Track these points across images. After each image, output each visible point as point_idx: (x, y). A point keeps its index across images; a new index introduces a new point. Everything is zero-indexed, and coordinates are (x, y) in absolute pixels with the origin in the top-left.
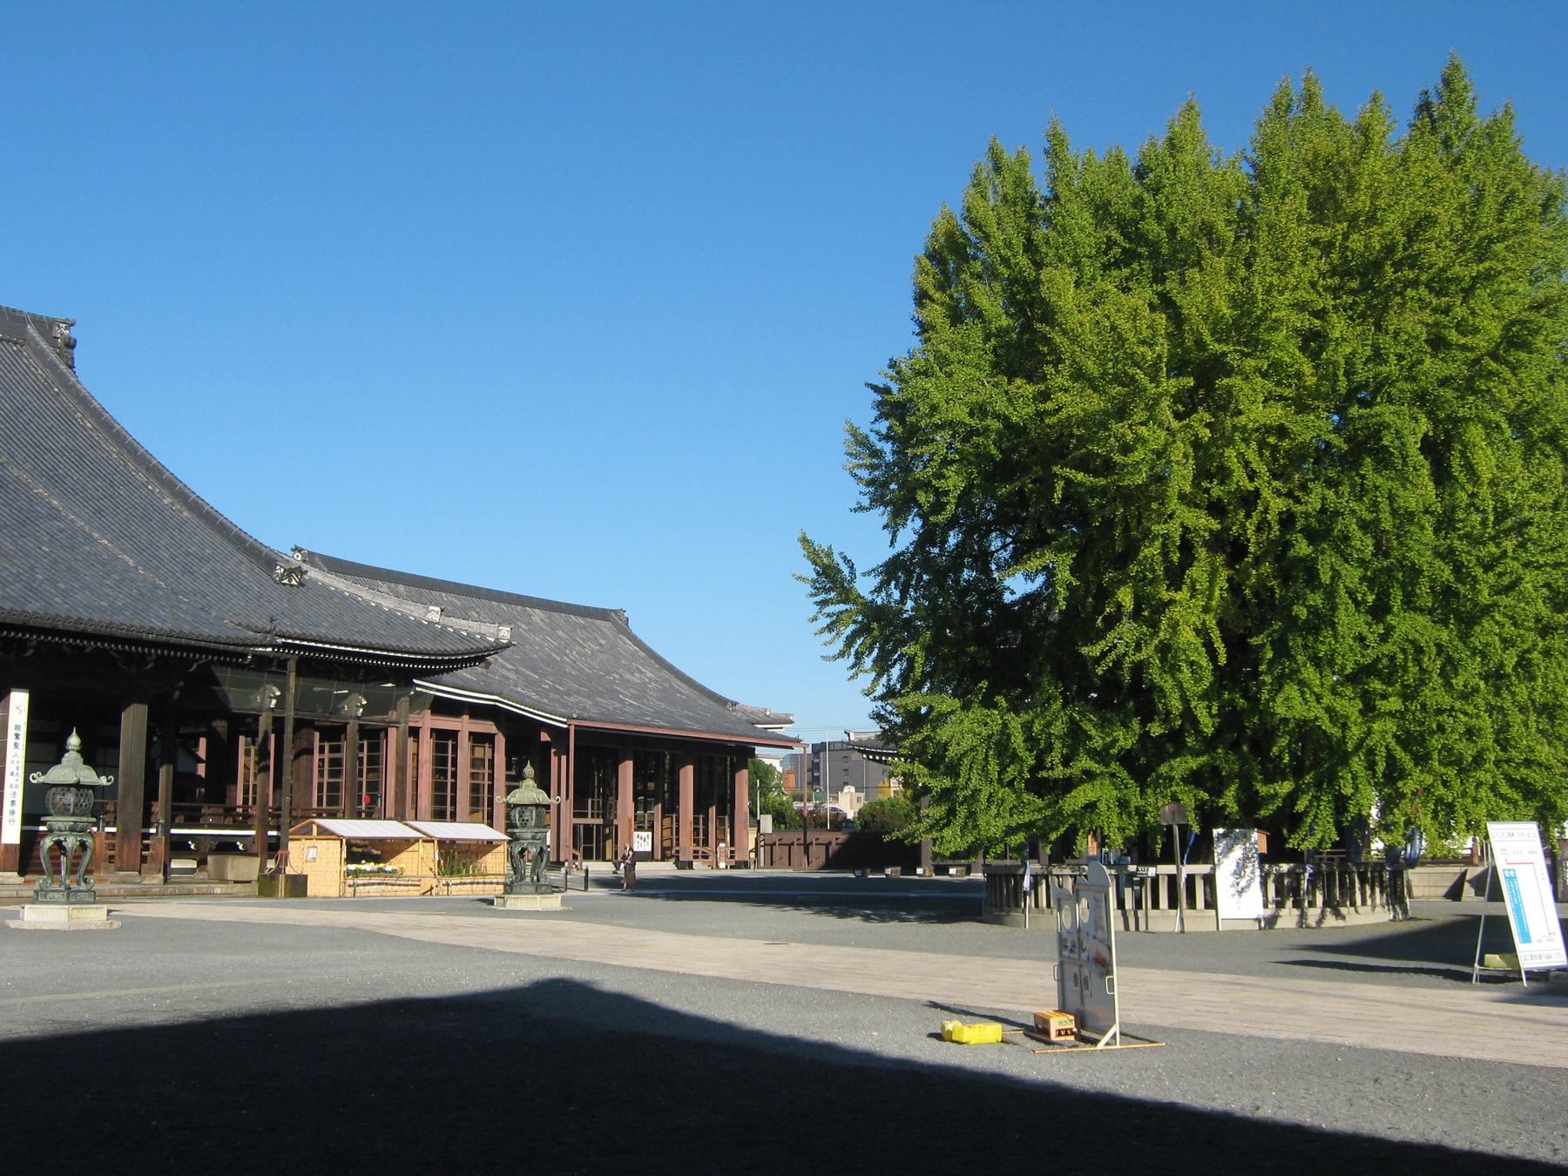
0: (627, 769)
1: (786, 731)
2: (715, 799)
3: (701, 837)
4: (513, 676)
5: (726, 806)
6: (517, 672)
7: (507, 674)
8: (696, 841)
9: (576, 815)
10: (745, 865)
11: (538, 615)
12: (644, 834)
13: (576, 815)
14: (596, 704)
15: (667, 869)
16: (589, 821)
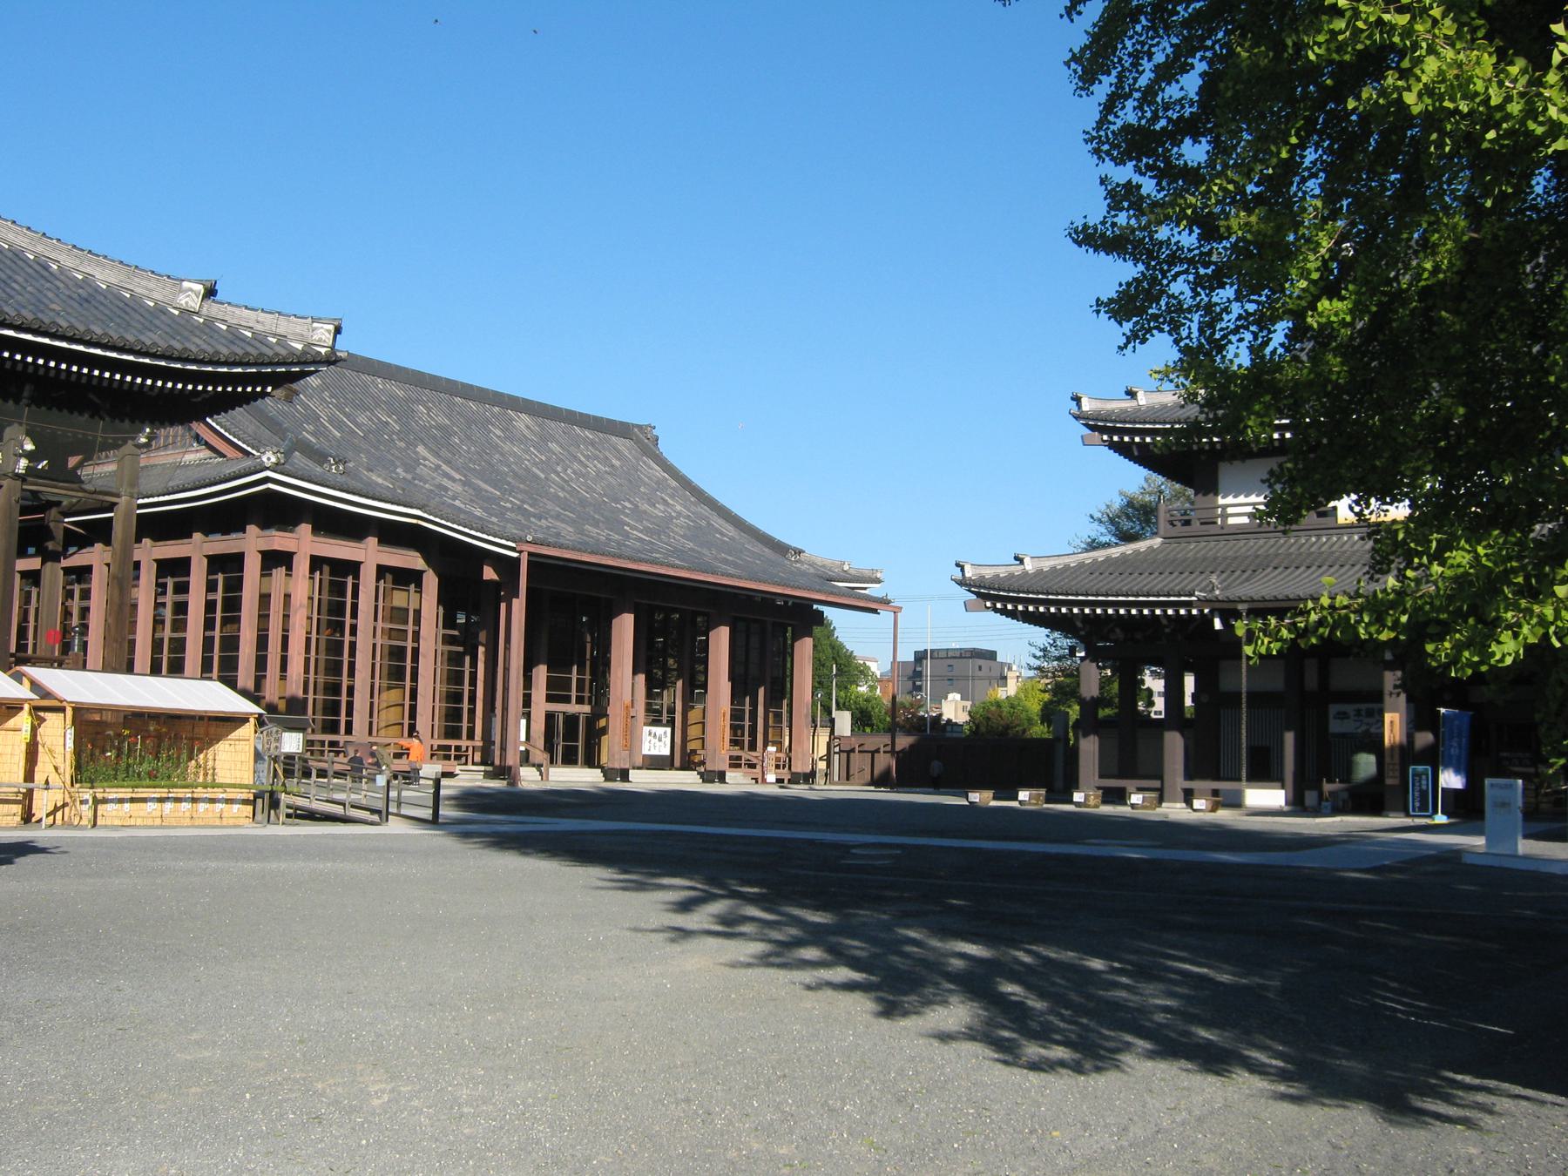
0: (624, 628)
1: (873, 590)
2: (763, 677)
3: (743, 735)
4: (459, 488)
5: (780, 690)
6: (464, 484)
7: (446, 482)
8: (734, 743)
9: (550, 699)
10: (809, 777)
11: (523, 421)
12: (659, 730)
13: (550, 699)
14: (582, 532)
15: (687, 781)
16: (573, 708)
